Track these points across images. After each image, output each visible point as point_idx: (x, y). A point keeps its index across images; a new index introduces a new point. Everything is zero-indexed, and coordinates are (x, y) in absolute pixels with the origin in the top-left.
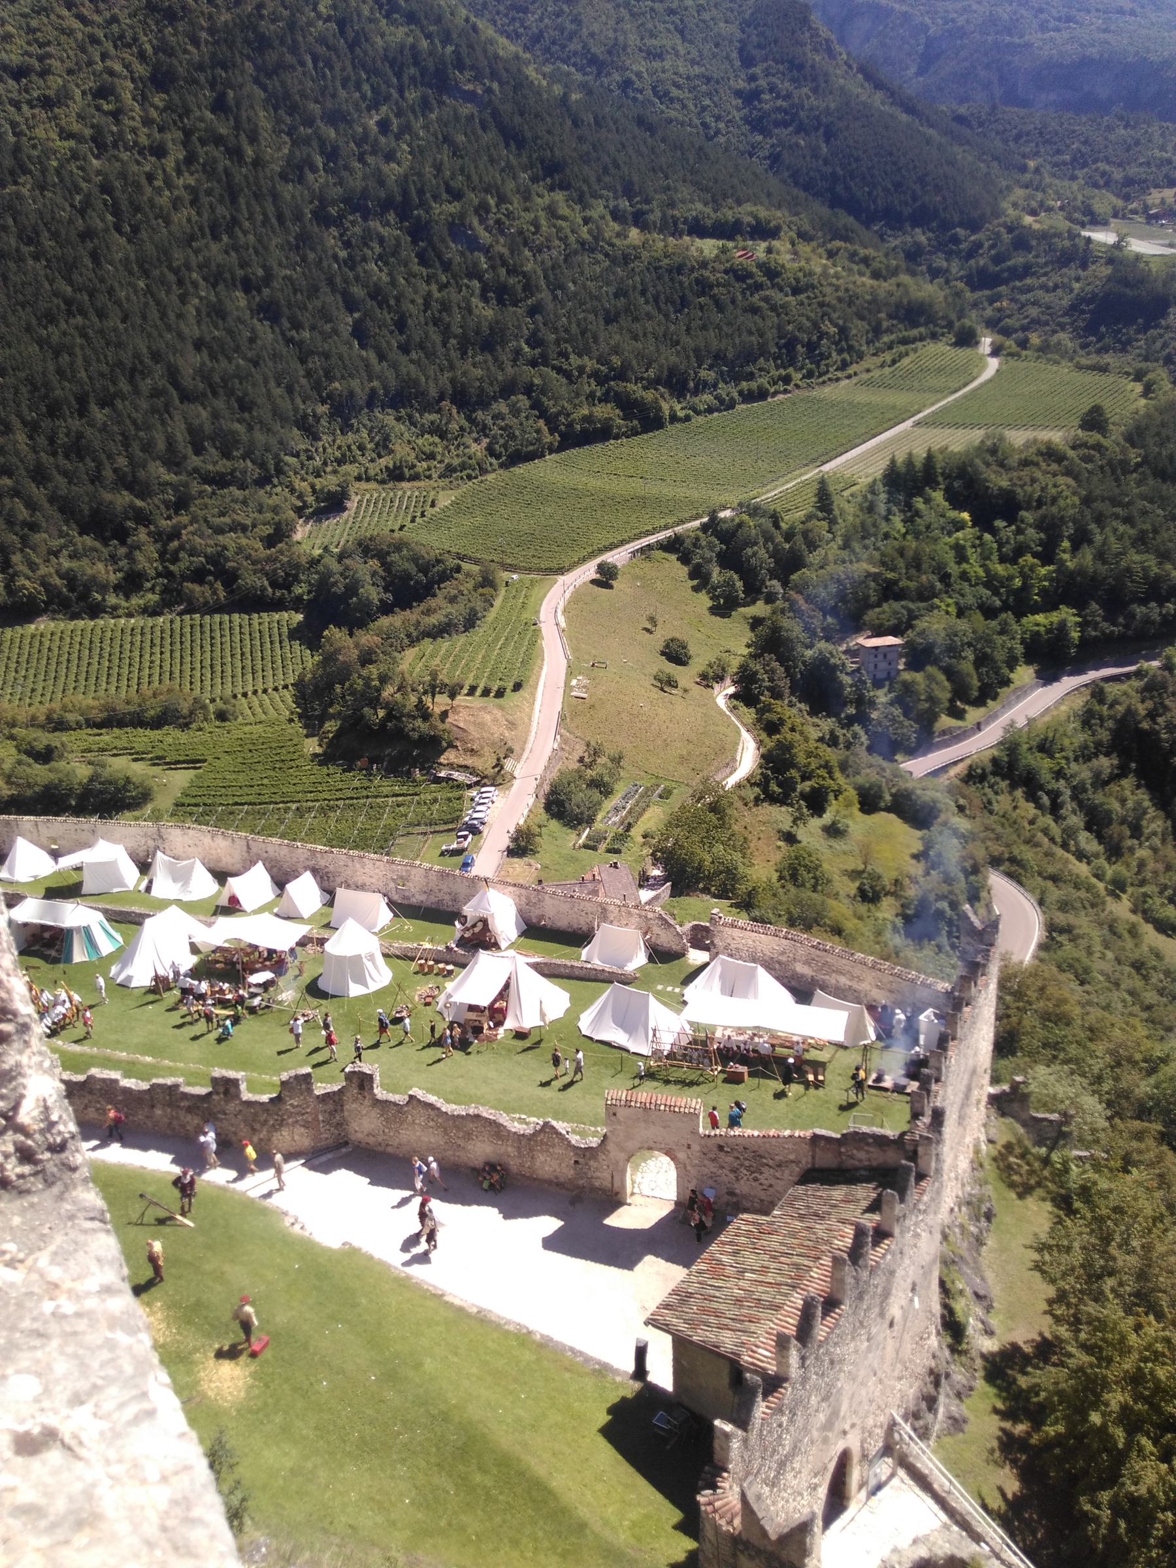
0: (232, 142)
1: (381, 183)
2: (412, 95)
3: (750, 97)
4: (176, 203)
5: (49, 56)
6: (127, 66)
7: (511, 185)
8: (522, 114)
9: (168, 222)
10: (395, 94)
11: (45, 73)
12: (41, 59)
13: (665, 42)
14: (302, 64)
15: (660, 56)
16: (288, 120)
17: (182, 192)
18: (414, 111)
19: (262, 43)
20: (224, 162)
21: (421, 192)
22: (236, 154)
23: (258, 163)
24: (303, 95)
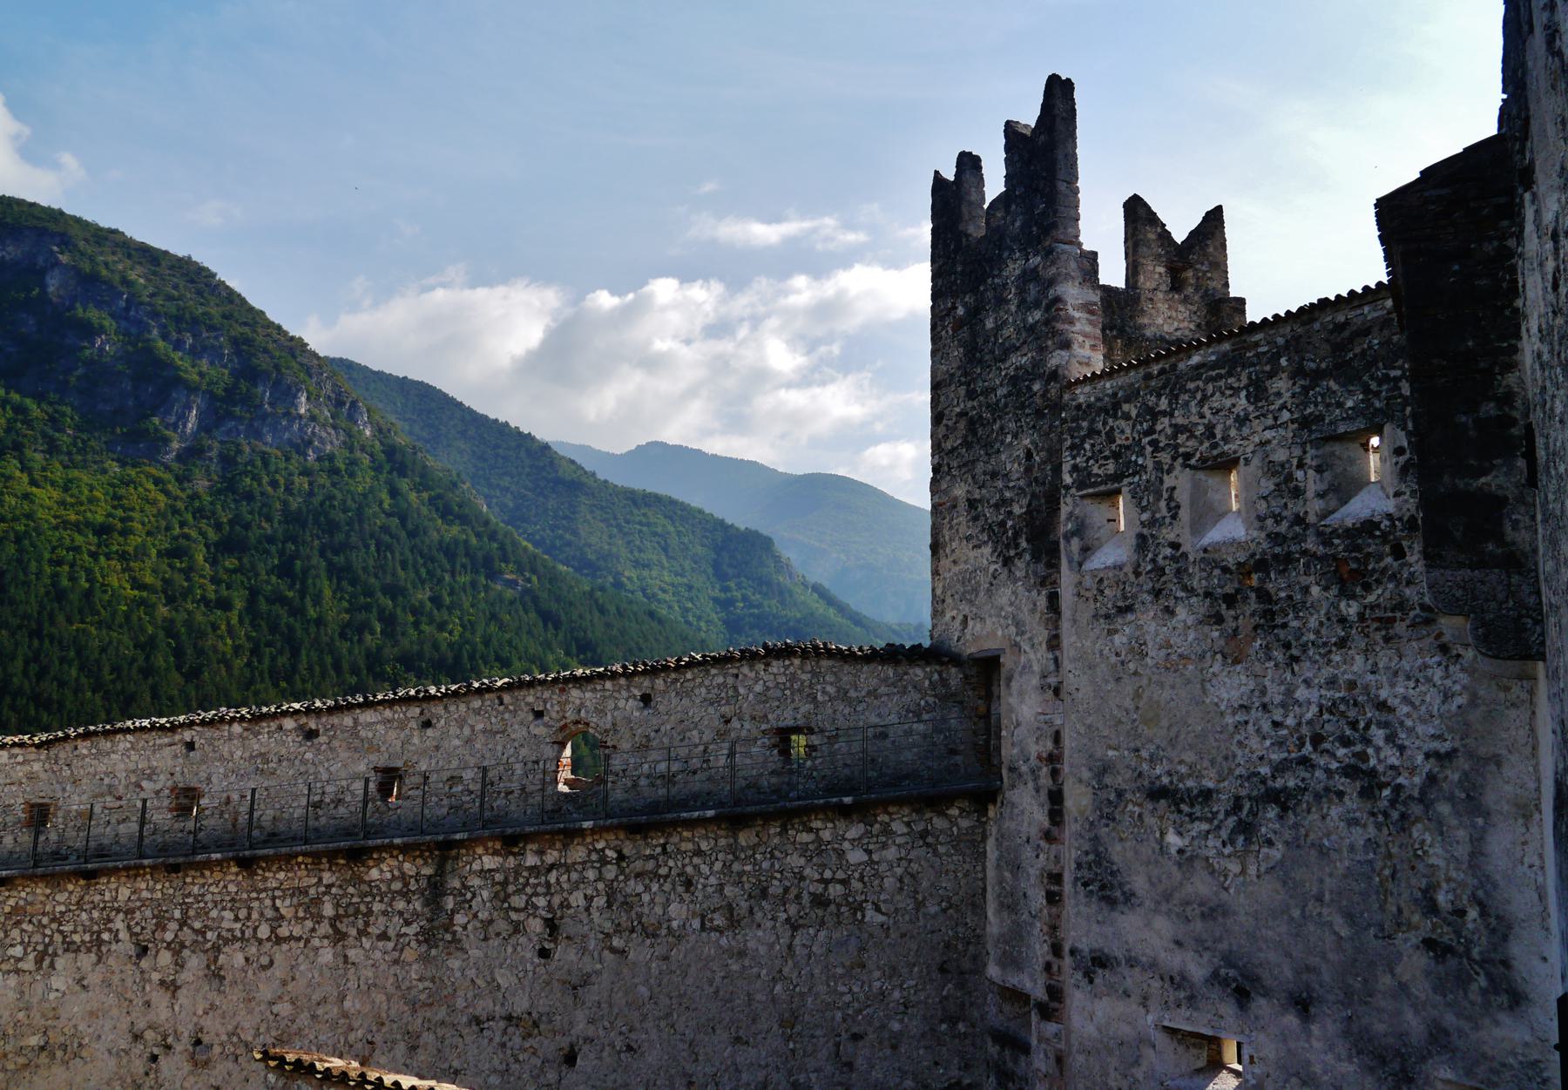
0: (297, 601)
1: (436, 646)
2: (463, 579)
3: (725, 604)
4: (237, 649)
5: (131, 519)
6: (203, 534)
7: (551, 657)
9: (229, 668)
10: (447, 578)
11: (125, 533)
12: (122, 520)
13: (650, 556)
14: (367, 547)
15: (647, 566)
16: (350, 589)
17: (242, 641)
18: (465, 591)
19: (332, 527)
20: (285, 618)
21: (472, 657)
22: (297, 612)
23: (319, 622)
24: (365, 569)
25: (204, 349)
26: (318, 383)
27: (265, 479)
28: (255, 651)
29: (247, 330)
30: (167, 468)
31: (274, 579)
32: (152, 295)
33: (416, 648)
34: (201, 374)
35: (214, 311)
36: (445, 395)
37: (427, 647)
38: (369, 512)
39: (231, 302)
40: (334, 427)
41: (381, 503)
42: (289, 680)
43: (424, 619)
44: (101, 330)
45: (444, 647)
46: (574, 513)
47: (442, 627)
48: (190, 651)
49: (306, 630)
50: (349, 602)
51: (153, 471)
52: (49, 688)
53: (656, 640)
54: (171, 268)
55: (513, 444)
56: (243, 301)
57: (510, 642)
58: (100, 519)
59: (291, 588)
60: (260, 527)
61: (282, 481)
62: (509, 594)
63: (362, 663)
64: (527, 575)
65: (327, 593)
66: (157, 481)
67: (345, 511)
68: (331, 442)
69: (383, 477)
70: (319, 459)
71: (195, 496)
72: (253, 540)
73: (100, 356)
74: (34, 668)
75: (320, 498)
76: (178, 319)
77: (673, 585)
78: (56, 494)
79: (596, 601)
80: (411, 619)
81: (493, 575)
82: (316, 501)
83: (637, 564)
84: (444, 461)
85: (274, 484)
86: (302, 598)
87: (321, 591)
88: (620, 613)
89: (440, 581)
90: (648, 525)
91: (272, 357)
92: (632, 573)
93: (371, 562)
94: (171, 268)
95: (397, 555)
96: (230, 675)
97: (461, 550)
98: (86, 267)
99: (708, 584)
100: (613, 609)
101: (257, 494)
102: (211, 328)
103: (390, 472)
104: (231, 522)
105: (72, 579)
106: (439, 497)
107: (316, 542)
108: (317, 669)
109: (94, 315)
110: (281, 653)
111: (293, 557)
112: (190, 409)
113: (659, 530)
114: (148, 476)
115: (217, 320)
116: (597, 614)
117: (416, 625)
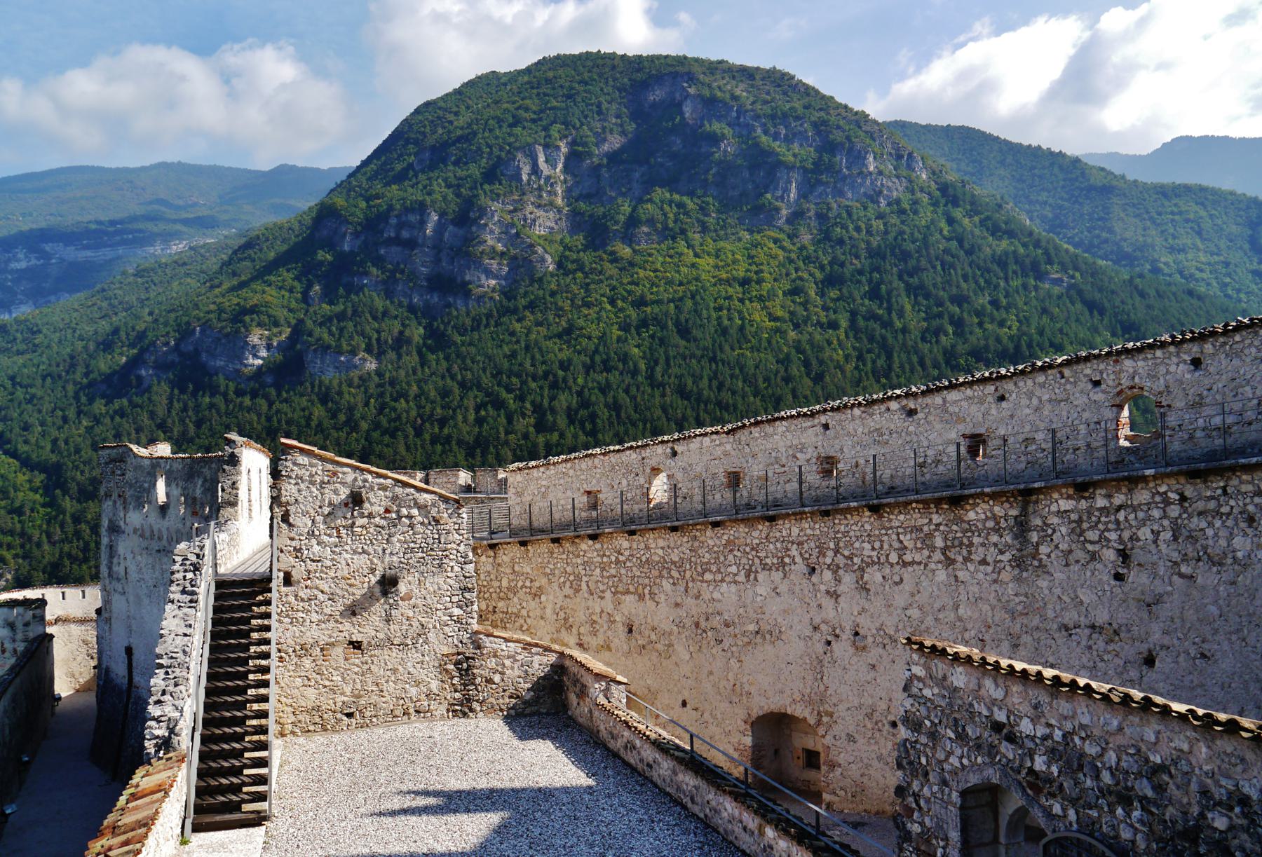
0: (886, 317)
1: (998, 340)
2: (1016, 283)
4: (847, 358)
5: (762, 271)
6: (811, 275)
8: (1100, 290)
9: (843, 372)
10: (1002, 284)
11: (759, 282)
12: (756, 273)
14: (934, 267)
15: (1182, 250)
16: (925, 302)
17: (850, 351)
18: (1018, 292)
19: (905, 256)
21: (1030, 346)
22: (887, 324)
23: (905, 330)
24: (935, 285)
25: (795, 135)
26: (881, 144)
27: (851, 227)
28: (860, 357)
29: (822, 114)
30: (781, 230)
31: (867, 302)
32: (753, 103)
33: (982, 342)
34: (795, 155)
35: (798, 105)
36: (984, 133)
37: (991, 342)
38: (932, 239)
39: (808, 95)
40: (898, 177)
41: (941, 231)
42: (887, 376)
43: (986, 319)
44: (724, 137)
45: (1005, 340)
46: (1108, 214)
47: (1002, 324)
48: (814, 362)
49: (896, 338)
50: (926, 312)
51: (772, 234)
52: (726, 396)
53: (1197, 315)
54: (763, 79)
55: (1047, 164)
56: (817, 92)
57: (1061, 331)
58: (741, 274)
59: (880, 307)
60: (852, 264)
61: (863, 226)
62: (1057, 290)
63: (940, 358)
64: (1071, 272)
65: (908, 307)
66: (776, 241)
67: (913, 242)
68: (897, 189)
69: (940, 211)
70: (889, 204)
71: (803, 248)
72: (848, 275)
73: (725, 156)
74: (715, 383)
75: (893, 234)
76: (773, 117)
77: (1209, 264)
78: (711, 261)
79: (1136, 288)
80: (976, 320)
81: (1040, 276)
82: (891, 237)
83: (1172, 250)
84: (987, 189)
85: (858, 229)
86: (890, 313)
87: (903, 307)
88: (1160, 295)
89: (996, 287)
90: (1180, 213)
91: (844, 131)
92: (1170, 259)
93: (939, 279)
94: (763, 79)
95: (959, 272)
96: (845, 377)
97: (1011, 260)
98: (707, 93)
99: (1246, 259)
100: (1152, 293)
101: (846, 239)
102: (797, 118)
103: (946, 205)
104: (831, 263)
105: (730, 319)
106: (988, 218)
107: (895, 269)
108: (907, 366)
109: (717, 127)
110: (879, 356)
111: (879, 284)
112: (790, 183)
113: (1192, 216)
114: (769, 238)
115: (800, 111)
116: (1138, 299)
117: (980, 324)
